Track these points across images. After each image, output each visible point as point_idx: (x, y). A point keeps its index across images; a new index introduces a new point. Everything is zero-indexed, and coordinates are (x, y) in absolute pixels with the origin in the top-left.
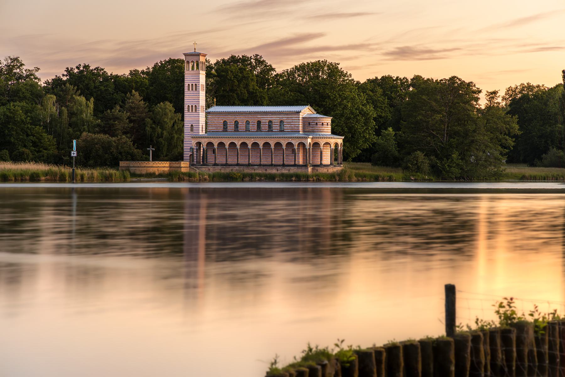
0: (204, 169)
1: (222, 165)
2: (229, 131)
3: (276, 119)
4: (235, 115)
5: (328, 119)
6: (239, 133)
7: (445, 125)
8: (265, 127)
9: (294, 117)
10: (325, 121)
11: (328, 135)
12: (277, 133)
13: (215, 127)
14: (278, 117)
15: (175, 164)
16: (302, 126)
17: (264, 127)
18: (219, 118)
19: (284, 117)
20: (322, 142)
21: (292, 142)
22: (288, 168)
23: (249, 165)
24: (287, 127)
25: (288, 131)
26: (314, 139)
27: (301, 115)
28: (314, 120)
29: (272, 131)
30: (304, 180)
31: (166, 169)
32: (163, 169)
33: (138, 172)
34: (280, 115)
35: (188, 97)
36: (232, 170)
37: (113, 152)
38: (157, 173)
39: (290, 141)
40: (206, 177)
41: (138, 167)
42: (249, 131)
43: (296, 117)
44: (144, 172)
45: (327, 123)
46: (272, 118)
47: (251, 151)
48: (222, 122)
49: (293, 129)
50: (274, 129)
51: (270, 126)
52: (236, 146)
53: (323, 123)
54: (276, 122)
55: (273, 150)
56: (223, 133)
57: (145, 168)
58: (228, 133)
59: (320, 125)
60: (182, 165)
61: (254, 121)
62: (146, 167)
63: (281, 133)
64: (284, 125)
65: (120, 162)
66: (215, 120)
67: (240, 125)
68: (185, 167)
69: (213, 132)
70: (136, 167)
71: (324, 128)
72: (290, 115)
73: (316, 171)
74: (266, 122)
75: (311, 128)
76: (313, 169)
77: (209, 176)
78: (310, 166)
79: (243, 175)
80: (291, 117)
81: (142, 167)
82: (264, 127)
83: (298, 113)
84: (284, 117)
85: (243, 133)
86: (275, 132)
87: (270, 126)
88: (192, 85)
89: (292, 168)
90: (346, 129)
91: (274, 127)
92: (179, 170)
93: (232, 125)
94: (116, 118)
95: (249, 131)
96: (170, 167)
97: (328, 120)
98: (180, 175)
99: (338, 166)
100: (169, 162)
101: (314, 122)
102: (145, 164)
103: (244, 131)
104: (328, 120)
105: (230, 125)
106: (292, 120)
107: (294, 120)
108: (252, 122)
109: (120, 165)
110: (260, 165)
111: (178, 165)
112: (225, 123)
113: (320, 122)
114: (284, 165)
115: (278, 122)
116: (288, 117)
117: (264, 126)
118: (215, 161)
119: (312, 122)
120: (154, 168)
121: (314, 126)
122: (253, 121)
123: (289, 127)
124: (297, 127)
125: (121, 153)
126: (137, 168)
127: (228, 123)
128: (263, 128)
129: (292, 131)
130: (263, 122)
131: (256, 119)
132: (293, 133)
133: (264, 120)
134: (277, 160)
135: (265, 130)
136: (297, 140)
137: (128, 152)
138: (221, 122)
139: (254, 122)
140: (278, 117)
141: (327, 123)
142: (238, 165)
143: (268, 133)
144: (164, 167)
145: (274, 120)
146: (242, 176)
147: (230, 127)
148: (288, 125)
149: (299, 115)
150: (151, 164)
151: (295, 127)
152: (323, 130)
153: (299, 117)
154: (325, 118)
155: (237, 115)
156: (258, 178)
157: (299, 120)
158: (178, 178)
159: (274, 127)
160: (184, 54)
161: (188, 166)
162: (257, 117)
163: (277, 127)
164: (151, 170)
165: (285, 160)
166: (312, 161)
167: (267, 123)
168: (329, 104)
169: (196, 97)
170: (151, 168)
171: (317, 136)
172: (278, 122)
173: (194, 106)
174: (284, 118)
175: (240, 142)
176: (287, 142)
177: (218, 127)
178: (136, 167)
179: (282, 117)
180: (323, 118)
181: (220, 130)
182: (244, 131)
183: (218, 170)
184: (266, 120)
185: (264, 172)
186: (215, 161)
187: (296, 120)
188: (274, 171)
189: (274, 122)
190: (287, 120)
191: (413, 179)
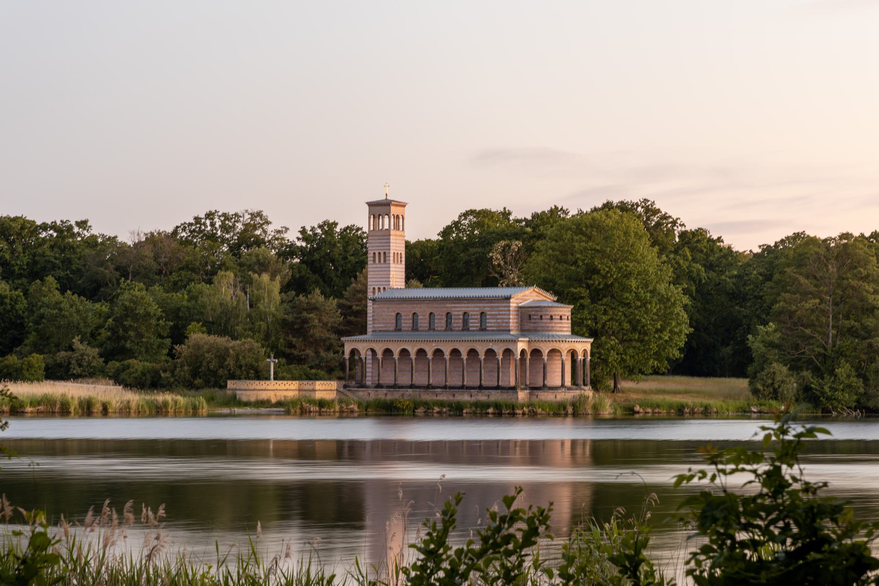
0: (361, 394)
1: (388, 387)
2: (404, 331)
3: (474, 310)
4: (412, 304)
5: (561, 309)
6: (419, 333)
7: (829, 317)
8: (457, 323)
9: (502, 307)
10: (557, 313)
11: (564, 336)
12: (476, 333)
13: (383, 323)
14: (477, 307)
15: (307, 385)
16: (515, 321)
17: (457, 323)
20: (545, 349)
21: (493, 348)
22: (487, 392)
23: (429, 387)
24: (491, 323)
25: (492, 330)
26: (532, 344)
27: (513, 304)
28: (537, 311)
29: (468, 330)
30: (508, 414)
31: (290, 394)
32: (285, 393)
33: (244, 399)
34: (480, 303)
35: (373, 273)
36: (403, 395)
37: (229, 364)
38: (274, 401)
39: (490, 347)
40: (352, 406)
41: (245, 390)
42: (434, 330)
43: (505, 307)
44: (253, 399)
45: (561, 317)
46: (468, 307)
47: (433, 363)
49: (499, 326)
50: (472, 327)
51: (465, 322)
52: (410, 355)
53: (551, 316)
54: (474, 315)
55: (465, 362)
56: (395, 333)
57: (255, 392)
58: (403, 333)
59: (547, 319)
60: (317, 387)
63: (481, 333)
64: (486, 319)
65: (229, 382)
67: (421, 319)
68: (325, 390)
69: (380, 331)
71: (553, 325)
72: (495, 303)
73: (535, 397)
74: (459, 315)
75: (532, 325)
76: (530, 394)
77: (360, 405)
78: (522, 389)
79: (415, 404)
80: (496, 307)
81: (251, 390)
82: (457, 323)
83: (508, 298)
85: (424, 333)
86: (473, 331)
87: (465, 322)
88: (379, 253)
89: (493, 392)
90: (626, 326)
91: (472, 323)
92: (312, 394)
93: (409, 319)
94: (313, 308)
95: (434, 330)
96: (300, 390)
97: (566, 311)
98: (303, 403)
99: (576, 389)
100: (297, 382)
101: (537, 315)
102: (263, 384)
103: (426, 331)
104: (566, 311)
105: (406, 319)
106: (499, 311)
107: (502, 311)
109: (228, 387)
110: (445, 387)
111: (311, 388)
113: (548, 315)
114: (481, 388)
115: (477, 315)
116: (492, 307)
118: (379, 380)
119: (534, 315)
120: (269, 392)
121: (537, 321)
122: (440, 312)
123: (494, 323)
124: (506, 323)
125: (240, 367)
127: (403, 317)
128: (455, 325)
129: (499, 330)
130: (455, 315)
131: (445, 309)
132: (500, 332)
134: (436, 379)
136: (501, 344)
137: (251, 366)
138: (392, 316)
139: (442, 315)
140: (477, 307)
141: (561, 317)
142: (412, 386)
143: (462, 333)
144: (287, 390)
145: (474, 311)
146: (412, 406)
147: (406, 323)
148: (493, 319)
149: (510, 303)
150: (272, 384)
151: (503, 323)
152: (552, 327)
153: (509, 307)
154: (561, 307)
155: (416, 304)
156: (437, 409)
157: (509, 311)
158: (301, 409)
159: (472, 323)
160: (367, 203)
161: (333, 388)
162: (445, 307)
163: (473, 323)
164: (264, 396)
165: (483, 378)
166: (530, 380)
167: (461, 317)
168: (599, 284)
169: (385, 273)
170: (265, 392)
171: (543, 339)
173: (382, 288)
174: (486, 307)
175: (416, 349)
176: (486, 348)
177: (388, 323)
179: (484, 307)
180: (556, 307)
181: (392, 329)
182: (426, 331)
183: (382, 395)
184: (459, 311)
185: (451, 398)
186: (379, 380)
187: (505, 311)
188: (465, 397)
189: (472, 315)
191: (755, 410)
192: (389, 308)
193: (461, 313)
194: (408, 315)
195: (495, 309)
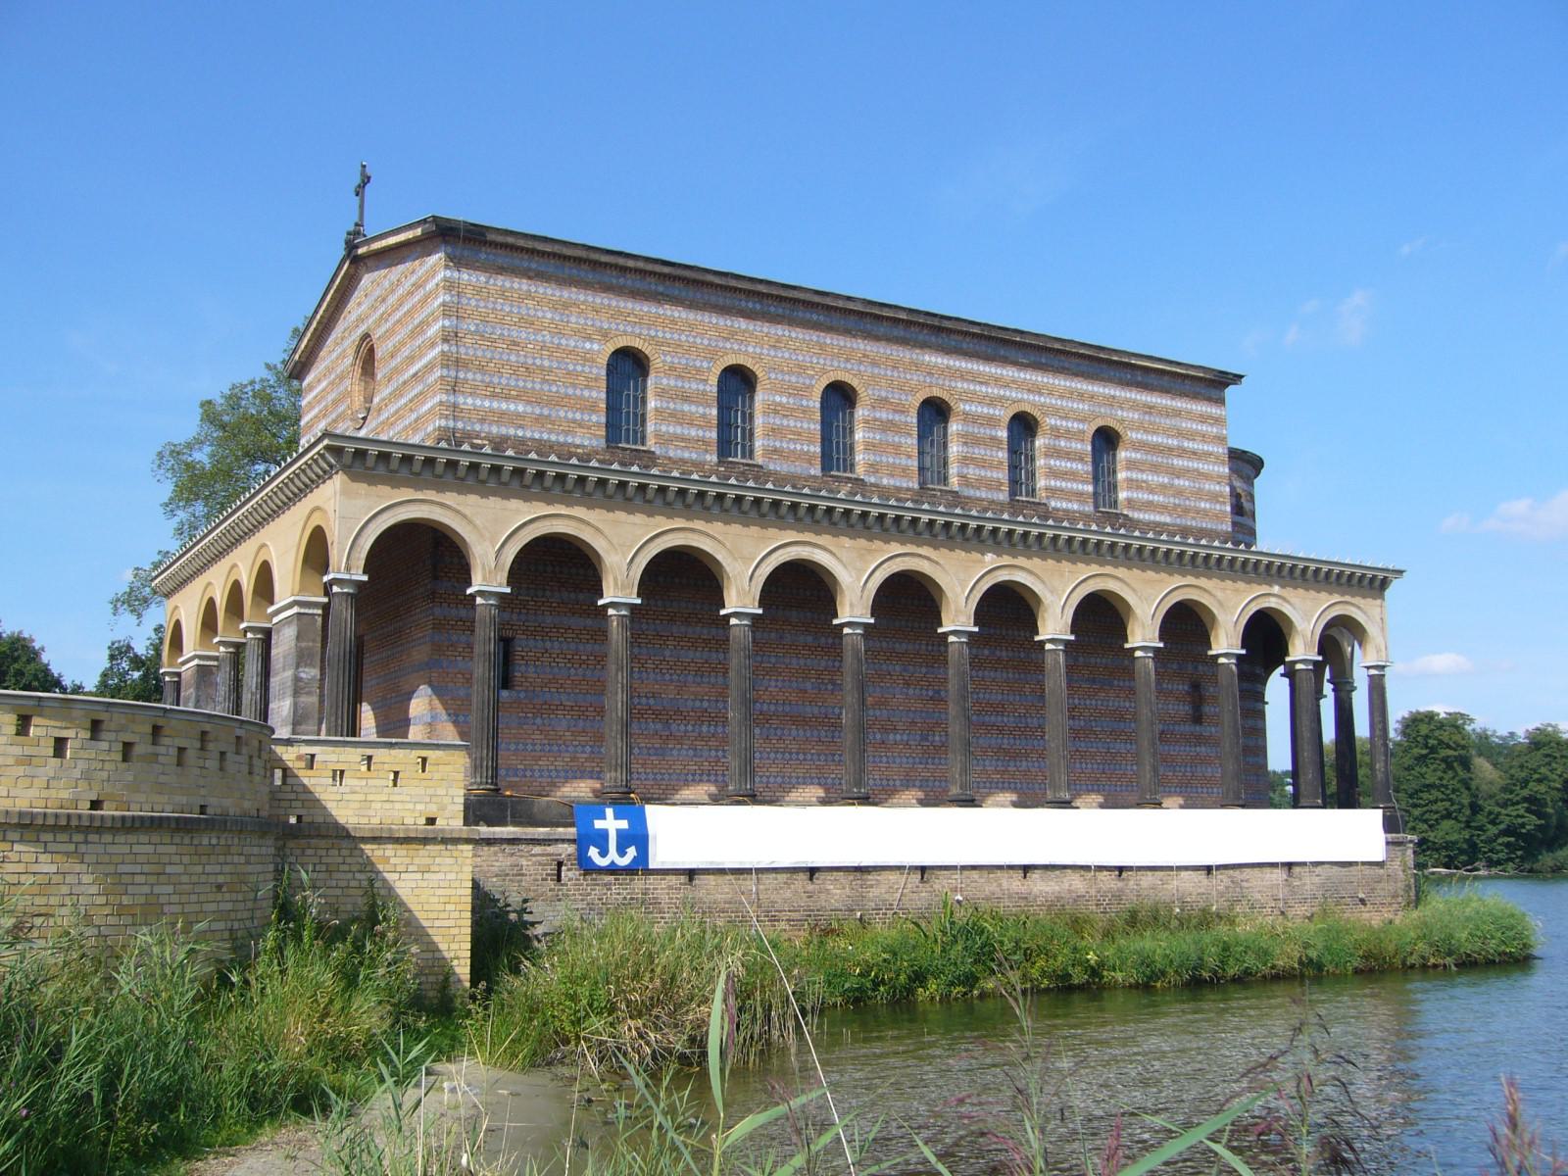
9: (1191, 416)
14: (1082, 396)
18: (566, 306)
19: (1121, 404)
46: (1036, 390)
48: (603, 360)
49: (1186, 510)
54: (1069, 435)
61: (895, 397)
74: (991, 421)
84: (1121, 404)
106: (1181, 434)
107: (1191, 436)
108: (882, 402)
112: (629, 366)
115: (1078, 436)
116: (1149, 409)
123: (1163, 488)
128: (972, 472)
131: (915, 378)
133: (983, 400)
135: (983, 494)
138: (587, 358)
139: (901, 410)
140: (1082, 396)
145: (1056, 412)
148: (1155, 468)
155: (749, 315)
162: (917, 366)
172: (1078, 436)
177: (557, 402)
184: (993, 401)
189: (1056, 432)
190: (1146, 431)
192: (566, 306)
193: (1005, 414)
194: (697, 374)
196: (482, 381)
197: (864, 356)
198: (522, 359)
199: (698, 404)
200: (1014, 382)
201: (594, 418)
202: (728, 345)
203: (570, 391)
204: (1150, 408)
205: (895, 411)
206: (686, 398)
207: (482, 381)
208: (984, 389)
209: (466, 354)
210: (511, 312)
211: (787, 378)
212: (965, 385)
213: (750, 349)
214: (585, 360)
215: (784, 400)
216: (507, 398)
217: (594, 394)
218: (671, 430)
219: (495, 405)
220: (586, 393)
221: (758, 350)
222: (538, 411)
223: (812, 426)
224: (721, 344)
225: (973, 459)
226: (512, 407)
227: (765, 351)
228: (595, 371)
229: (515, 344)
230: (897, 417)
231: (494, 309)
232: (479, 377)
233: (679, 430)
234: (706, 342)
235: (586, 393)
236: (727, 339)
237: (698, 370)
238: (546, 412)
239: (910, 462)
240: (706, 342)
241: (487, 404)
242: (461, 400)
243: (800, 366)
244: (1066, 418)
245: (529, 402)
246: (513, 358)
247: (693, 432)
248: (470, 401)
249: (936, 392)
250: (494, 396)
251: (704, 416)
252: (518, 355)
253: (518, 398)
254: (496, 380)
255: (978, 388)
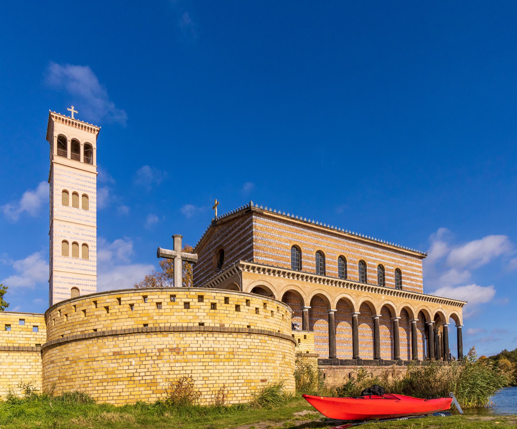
14: (393, 260)
18: (281, 233)
61: (354, 260)
62: (261, 333)
66: (272, 237)
70: (187, 330)
117: (371, 274)
126: (190, 339)
131: (358, 255)
138: (286, 247)
139: (355, 263)
140: (393, 260)
178: (187, 330)
184: (374, 261)
193: (376, 264)
195: (410, 267)
196: (263, 253)
197: (347, 249)
198: (272, 247)
199: (311, 260)
200: (379, 256)
201: (289, 263)
202: (318, 245)
203: (283, 256)
204: (407, 264)
205: (354, 263)
206: (309, 259)
207: (263, 253)
208: (372, 258)
209: (259, 245)
210: (269, 234)
211: (330, 254)
212: (368, 257)
213: (322, 246)
214: (286, 247)
215: (330, 260)
216: (269, 257)
217: (289, 257)
218: (306, 267)
219: (266, 259)
220: (287, 257)
221: (324, 246)
222: (276, 261)
223: (336, 267)
224: (316, 245)
225: (370, 276)
226: (270, 260)
227: (326, 247)
228: (288, 251)
229: (270, 243)
230: (354, 265)
231: (265, 233)
232: (262, 252)
233: (307, 267)
234: (313, 244)
235: (287, 257)
236: (317, 243)
237: (311, 251)
238: (278, 261)
239: (357, 276)
240: (313, 244)
241: (264, 259)
242: (259, 258)
243: (333, 251)
244: (389, 266)
245: (274, 259)
246: (270, 247)
247: (311, 268)
248: (261, 258)
249: (362, 259)
250: (266, 257)
251: (313, 263)
252: (271, 246)
253: (271, 257)
254: (266, 253)
255: (371, 258)
